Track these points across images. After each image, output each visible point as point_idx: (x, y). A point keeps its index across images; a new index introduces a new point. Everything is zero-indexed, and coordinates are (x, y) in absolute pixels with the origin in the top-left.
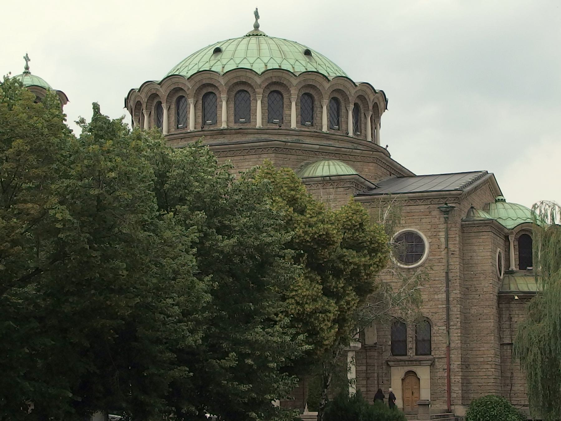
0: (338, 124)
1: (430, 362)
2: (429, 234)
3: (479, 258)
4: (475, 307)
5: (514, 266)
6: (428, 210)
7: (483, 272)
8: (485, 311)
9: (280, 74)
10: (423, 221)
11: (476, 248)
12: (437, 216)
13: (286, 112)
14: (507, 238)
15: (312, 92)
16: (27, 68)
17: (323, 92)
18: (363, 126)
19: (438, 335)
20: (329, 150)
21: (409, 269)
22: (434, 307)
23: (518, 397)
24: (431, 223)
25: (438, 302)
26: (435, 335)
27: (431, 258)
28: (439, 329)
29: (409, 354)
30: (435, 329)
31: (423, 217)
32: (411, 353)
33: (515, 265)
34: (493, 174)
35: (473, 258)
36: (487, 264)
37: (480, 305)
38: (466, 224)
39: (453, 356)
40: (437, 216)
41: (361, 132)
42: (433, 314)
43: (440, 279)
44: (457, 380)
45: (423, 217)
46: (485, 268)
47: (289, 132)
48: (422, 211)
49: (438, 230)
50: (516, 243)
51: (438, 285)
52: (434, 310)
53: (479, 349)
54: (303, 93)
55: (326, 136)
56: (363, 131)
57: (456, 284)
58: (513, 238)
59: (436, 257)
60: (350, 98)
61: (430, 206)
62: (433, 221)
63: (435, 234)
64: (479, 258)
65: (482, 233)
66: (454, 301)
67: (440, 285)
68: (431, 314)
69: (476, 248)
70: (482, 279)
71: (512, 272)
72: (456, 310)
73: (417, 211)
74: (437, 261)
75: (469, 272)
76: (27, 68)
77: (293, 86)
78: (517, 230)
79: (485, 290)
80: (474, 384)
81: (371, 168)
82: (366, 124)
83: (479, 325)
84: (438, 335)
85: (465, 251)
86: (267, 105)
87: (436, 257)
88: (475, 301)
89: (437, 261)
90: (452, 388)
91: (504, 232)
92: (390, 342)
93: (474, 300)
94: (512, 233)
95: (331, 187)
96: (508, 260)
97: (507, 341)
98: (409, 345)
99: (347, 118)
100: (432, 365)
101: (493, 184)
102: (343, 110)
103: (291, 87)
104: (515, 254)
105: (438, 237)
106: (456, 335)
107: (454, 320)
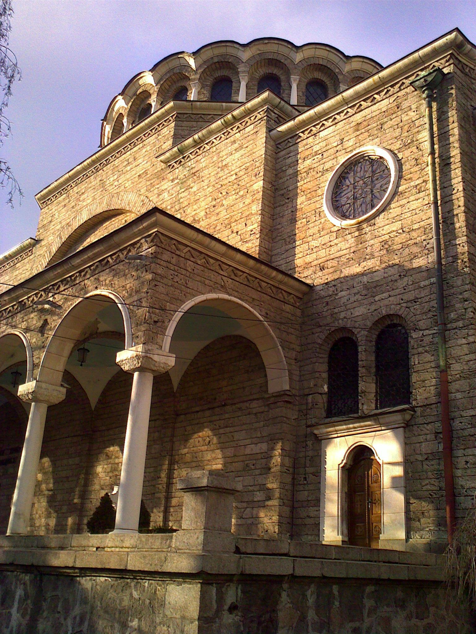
6: (395, 103)
12: (414, 107)
17: (290, 67)
19: (420, 349)
24: (401, 124)
25: (418, 276)
26: (415, 351)
31: (385, 120)
39: (459, 395)
40: (414, 107)
42: (409, 304)
45: (385, 120)
51: (419, 239)
52: (411, 296)
59: (412, 184)
60: (340, 77)
63: (409, 141)
67: (423, 238)
68: (405, 305)
72: (459, 282)
73: (374, 114)
74: (414, 191)
77: (243, 62)
84: (420, 349)
87: (412, 184)
89: (414, 191)
90: (461, 482)
92: (326, 388)
95: (237, 131)
106: (464, 341)
107: (458, 306)
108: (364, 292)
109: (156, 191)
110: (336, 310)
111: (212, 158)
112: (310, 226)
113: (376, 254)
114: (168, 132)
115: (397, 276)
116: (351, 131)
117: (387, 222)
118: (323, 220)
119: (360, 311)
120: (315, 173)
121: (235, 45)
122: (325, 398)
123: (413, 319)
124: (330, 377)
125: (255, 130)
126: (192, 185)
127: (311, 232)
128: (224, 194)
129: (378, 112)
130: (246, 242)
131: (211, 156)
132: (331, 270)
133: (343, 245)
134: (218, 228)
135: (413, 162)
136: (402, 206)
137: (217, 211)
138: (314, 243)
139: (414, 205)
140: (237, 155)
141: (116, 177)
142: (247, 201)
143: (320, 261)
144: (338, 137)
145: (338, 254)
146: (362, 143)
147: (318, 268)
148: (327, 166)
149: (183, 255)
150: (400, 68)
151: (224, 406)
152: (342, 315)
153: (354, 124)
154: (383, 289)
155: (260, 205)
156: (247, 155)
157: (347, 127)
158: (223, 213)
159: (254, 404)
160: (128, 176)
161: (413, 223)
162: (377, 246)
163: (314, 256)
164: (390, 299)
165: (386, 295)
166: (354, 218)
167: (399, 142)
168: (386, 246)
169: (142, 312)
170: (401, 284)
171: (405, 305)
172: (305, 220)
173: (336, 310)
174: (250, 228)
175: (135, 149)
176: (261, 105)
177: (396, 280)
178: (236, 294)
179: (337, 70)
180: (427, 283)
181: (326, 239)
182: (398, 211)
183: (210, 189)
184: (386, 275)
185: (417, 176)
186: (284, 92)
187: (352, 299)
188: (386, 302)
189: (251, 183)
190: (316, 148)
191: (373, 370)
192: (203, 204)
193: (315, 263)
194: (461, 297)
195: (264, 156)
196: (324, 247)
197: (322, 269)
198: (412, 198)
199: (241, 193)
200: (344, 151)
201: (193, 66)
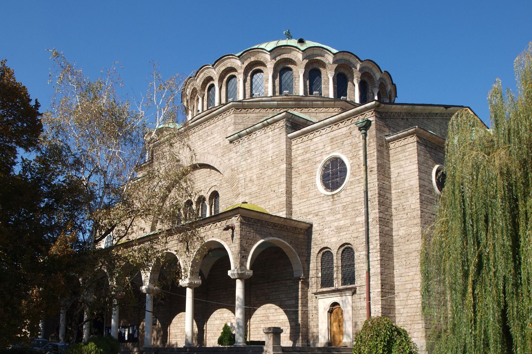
2: (350, 155)
3: (406, 173)
4: (403, 228)
6: (349, 131)
7: (409, 187)
8: (413, 231)
10: (345, 143)
11: (402, 163)
12: (358, 135)
19: (359, 261)
21: (333, 195)
25: (358, 226)
27: (351, 180)
28: (360, 255)
30: (356, 254)
31: (345, 139)
32: (338, 284)
35: (400, 174)
36: (414, 179)
37: (408, 224)
42: (354, 239)
43: (361, 200)
44: (377, 310)
45: (345, 139)
46: (411, 183)
48: (344, 133)
52: (355, 235)
53: (408, 274)
57: (375, 203)
59: (357, 178)
61: (351, 126)
62: (353, 141)
63: (355, 154)
64: (406, 173)
65: (407, 145)
66: (373, 222)
68: (353, 239)
69: (402, 163)
70: (409, 195)
72: (375, 232)
73: (339, 134)
74: (357, 182)
79: (412, 207)
80: (404, 315)
83: (407, 247)
87: (357, 178)
88: (403, 221)
89: (357, 182)
93: (402, 221)
95: (270, 130)
103: (267, 63)
105: (358, 156)
107: (374, 242)
108: (336, 231)
109: (227, 157)
110: (323, 238)
111: (258, 144)
112: (311, 191)
113: (341, 212)
114: (230, 120)
115: (349, 225)
116: (329, 141)
117: (345, 196)
118: (316, 190)
119: (334, 240)
120: (312, 162)
121: (264, 51)
123: (356, 246)
125: (280, 132)
126: (248, 158)
127: (310, 195)
128: (266, 167)
129: (341, 134)
130: (280, 197)
131: (257, 142)
132: (321, 217)
133: (326, 205)
134: (264, 187)
135: (357, 166)
137: (263, 177)
138: (313, 201)
139: (357, 189)
140: (271, 146)
141: (201, 142)
142: (278, 175)
143: (315, 211)
144: (323, 144)
145: (324, 209)
146: (334, 150)
147: (315, 215)
148: (318, 159)
149: (251, 223)
150: (351, 113)
151: (274, 281)
152: (326, 241)
153: (330, 138)
154: (344, 230)
155: (285, 177)
156: (277, 146)
157: (327, 139)
158: (266, 179)
160: (209, 144)
162: (341, 209)
163: (313, 208)
164: (347, 235)
165: (345, 233)
167: (351, 154)
168: (345, 209)
170: (351, 228)
171: (353, 239)
172: (307, 188)
173: (323, 238)
174: (280, 190)
175: (211, 126)
177: (349, 227)
178: (276, 235)
181: (318, 200)
183: (258, 163)
184: (345, 223)
186: (295, 79)
187: (330, 233)
188: (345, 237)
189: (280, 164)
190: (312, 148)
192: (255, 171)
194: (375, 238)
195: (285, 149)
196: (317, 204)
197: (317, 215)
198: (356, 186)
199: (275, 169)
200: (325, 153)
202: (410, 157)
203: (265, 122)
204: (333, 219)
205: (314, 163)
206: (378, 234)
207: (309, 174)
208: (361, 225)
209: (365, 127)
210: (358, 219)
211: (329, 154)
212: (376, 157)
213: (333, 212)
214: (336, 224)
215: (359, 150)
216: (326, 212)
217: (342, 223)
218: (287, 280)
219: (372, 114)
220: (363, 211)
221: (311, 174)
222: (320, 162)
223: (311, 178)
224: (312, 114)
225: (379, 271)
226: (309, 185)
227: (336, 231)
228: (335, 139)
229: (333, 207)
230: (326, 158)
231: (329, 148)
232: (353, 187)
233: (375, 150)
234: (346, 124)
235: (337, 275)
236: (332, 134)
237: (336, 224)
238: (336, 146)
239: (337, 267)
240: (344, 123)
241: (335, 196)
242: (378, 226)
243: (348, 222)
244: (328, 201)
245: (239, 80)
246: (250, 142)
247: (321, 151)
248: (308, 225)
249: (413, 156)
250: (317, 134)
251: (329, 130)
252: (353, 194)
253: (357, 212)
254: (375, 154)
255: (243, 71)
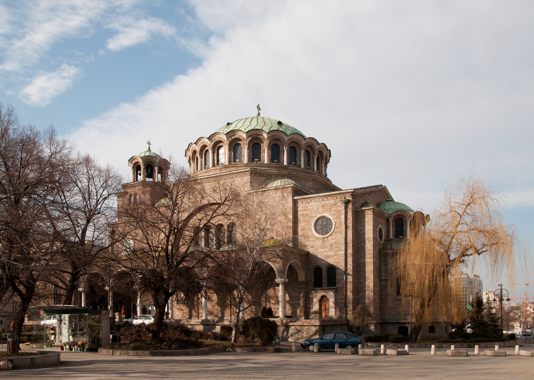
0: (295, 161)
1: (334, 290)
2: (335, 217)
5: (391, 236)
6: (335, 203)
9: (255, 132)
12: (340, 206)
13: (262, 154)
14: (388, 220)
15: (278, 143)
16: (149, 148)
18: (312, 163)
20: (284, 173)
21: (324, 237)
22: (337, 259)
23: (389, 310)
25: (340, 256)
29: (323, 286)
31: (332, 207)
33: (393, 236)
34: (385, 186)
36: (370, 234)
38: (358, 211)
40: (340, 206)
41: (310, 167)
43: (341, 242)
45: (332, 207)
47: (263, 165)
48: (332, 203)
49: (340, 214)
50: (394, 223)
52: (337, 261)
54: (273, 143)
55: (286, 168)
56: (312, 166)
57: (350, 245)
58: (392, 220)
59: (339, 230)
71: (391, 240)
72: (350, 260)
74: (339, 232)
75: (360, 239)
76: (149, 148)
78: (394, 215)
81: (311, 184)
82: (313, 162)
85: (358, 227)
86: (251, 151)
87: (339, 230)
89: (339, 232)
91: (386, 216)
92: (313, 280)
93: (362, 255)
94: (391, 217)
96: (388, 232)
97: (383, 278)
98: (324, 281)
99: (301, 158)
100: (336, 292)
101: (386, 192)
102: (298, 154)
104: (393, 230)
108: (325, 257)
110: (317, 260)
113: (328, 247)
114: (247, 179)
115: (334, 255)
116: (321, 206)
118: (312, 233)
122: (313, 283)
124: (314, 277)
129: (329, 203)
132: (315, 249)
133: (318, 242)
136: (336, 236)
139: (339, 236)
145: (317, 245)
148: (313, 215)
152: (318, 262)
153: (321, 204)
159: (293, 283)
161: (338, 241)
162: (328, 245)
163: (309, 243)
165: (331, 259)
166: (322, 235)
169: (222, 235)
170: (335, 257)
176: (291, 187)
179: (301, 143)
180: (342, 258)
182: (334, 237)
185: (340, 228)
190: (309, 208)
191: (327, 277)
193: (309, 245)
197: (312, 248)
198: (338, 234)
201: (245, 138)
202: (368, 221)
203: (278, 187)
204: (323, 250)
205: (310, 217)
206: (352, 262)
207: (307, 223)
208: (341, 256)
209: (347, 203)
210: (339, 253)
211: (321, 213)
212: (351, 220)
213: (323, 247)
214: (325, 254)
215: (341, 215)
216: (319, 247)
217: (329, 253)
218: (293, 282)
219: (350, 196)
220: (343, 248)
221: (309, 223)
222: (315, 217)
223: (309, 225)
224: (297, 181)
225: (352, 281)
226: (307, 229)
227: (325, 257)
228: (326, 206)
229: (323, 244)
230: (319, 216)
231: (321, 210)
232: (336, 235)
233: (351, 216)
234: (333, 198)
235: (325, 281)
236: (323, 202)
237: (325, 254)
238: (326, 209)
239: (325, 277)
240: (332, 197)
241: (325, 238)
242: (352, 257)
243: (333, 253)
244: (320, 240)
245: (244, 148)
246: (264, 197)
247: (315, 211)
248: (307, 253)
249: (370, 221)
250: (313, 200)
251: (321, 200)
252: (336, 239)
253: (339, 249)
254: (351, 218)
255: (248, 143)
